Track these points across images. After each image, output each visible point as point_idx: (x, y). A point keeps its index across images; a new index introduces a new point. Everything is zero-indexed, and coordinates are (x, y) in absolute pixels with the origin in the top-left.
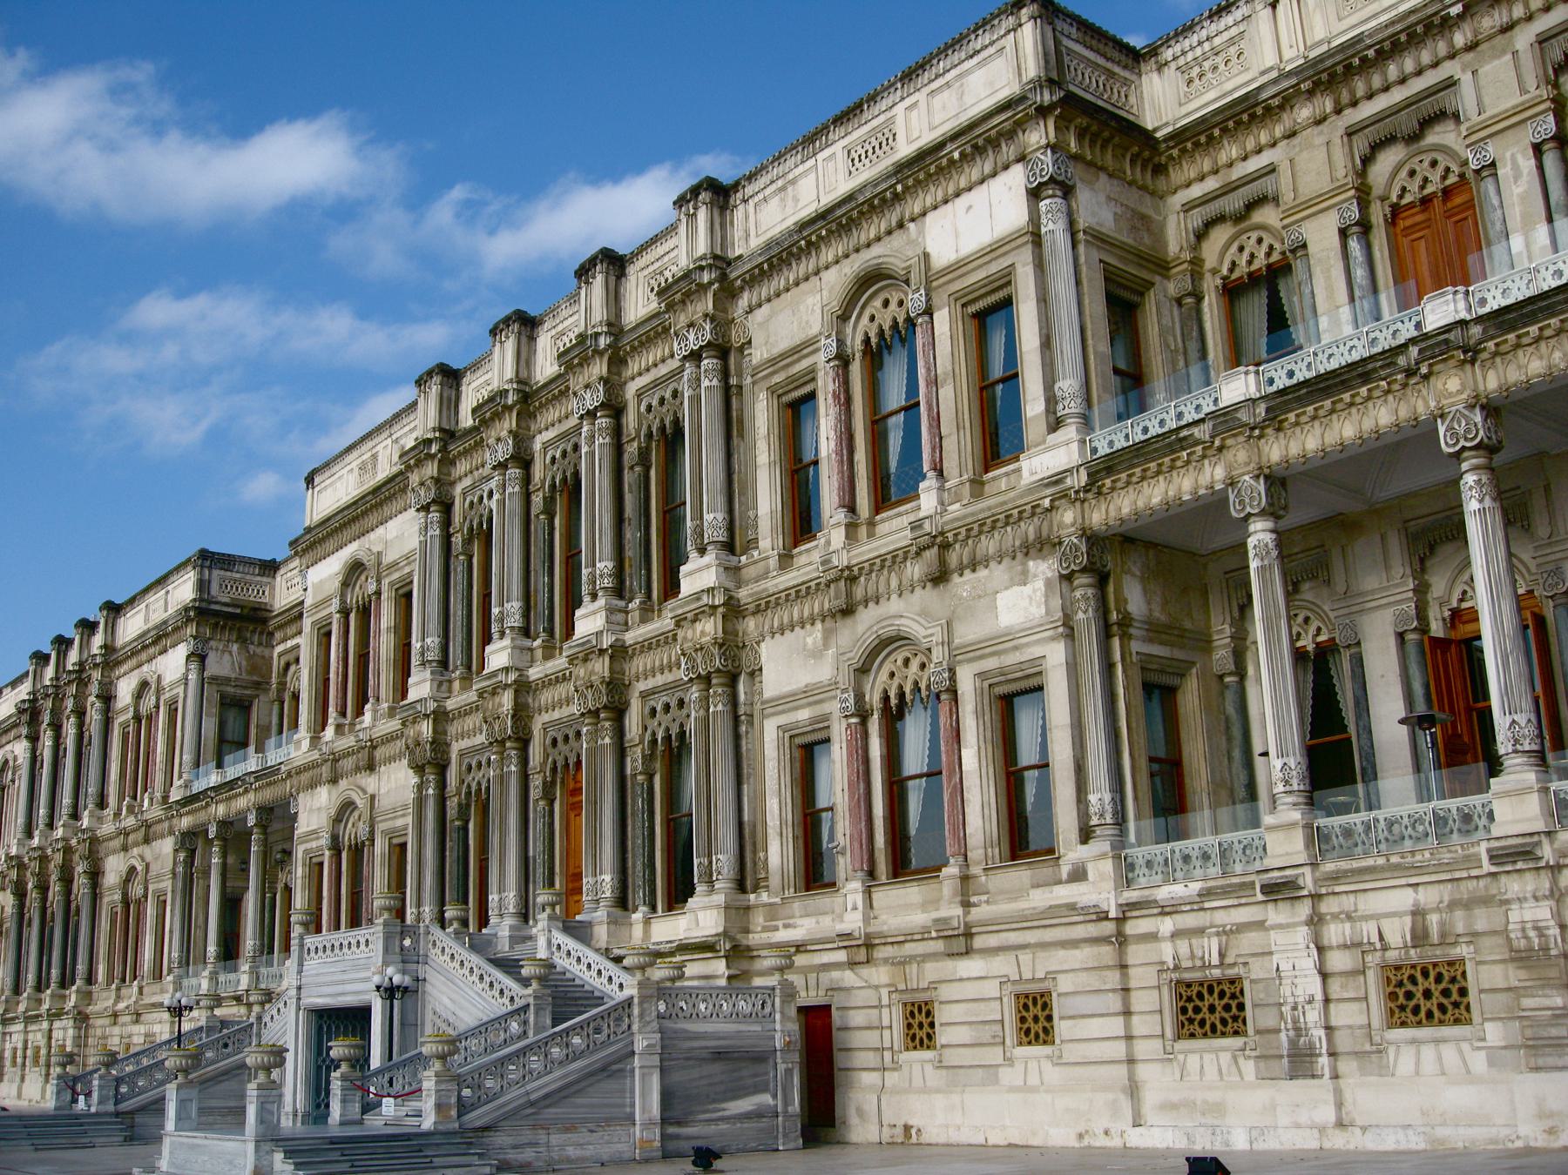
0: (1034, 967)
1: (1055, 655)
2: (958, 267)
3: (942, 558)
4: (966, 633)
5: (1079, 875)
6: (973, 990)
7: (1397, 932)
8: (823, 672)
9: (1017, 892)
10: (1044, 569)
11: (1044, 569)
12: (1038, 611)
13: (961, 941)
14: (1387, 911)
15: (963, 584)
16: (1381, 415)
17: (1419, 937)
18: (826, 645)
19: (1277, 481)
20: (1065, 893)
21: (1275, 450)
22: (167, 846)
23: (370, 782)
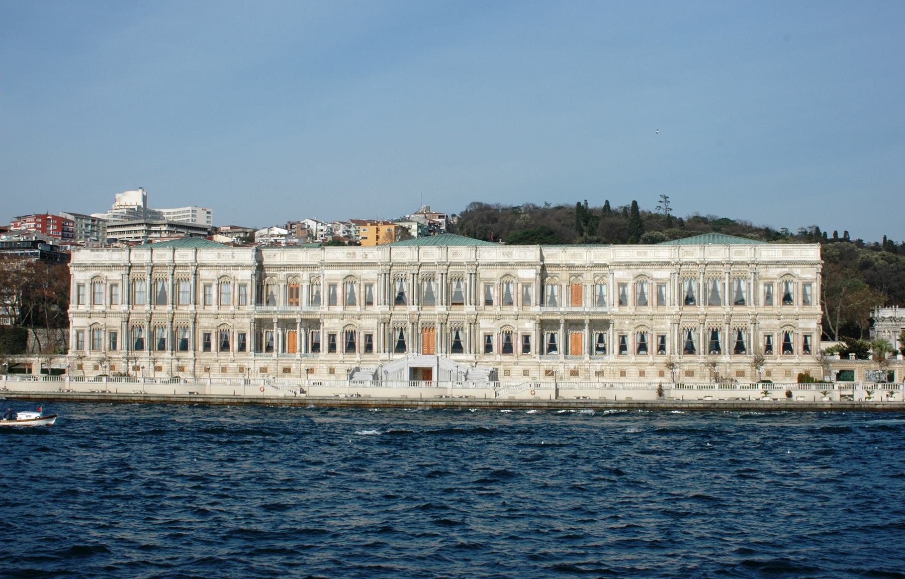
0: (526, 368)
1: (534, 333)
2: (523, 279)
3: (517, 317)
4: (520, 327)
6: (518, 369)
8: (493, 326)
9: (525, 358)
11: (533, 322)
13: (516, 364)
14: (572, 365)
16: (579, 317)
19: (566, 320)
20: (529, 360)
21: (566, 317)
22: (247, 321)
23: (359, 322)
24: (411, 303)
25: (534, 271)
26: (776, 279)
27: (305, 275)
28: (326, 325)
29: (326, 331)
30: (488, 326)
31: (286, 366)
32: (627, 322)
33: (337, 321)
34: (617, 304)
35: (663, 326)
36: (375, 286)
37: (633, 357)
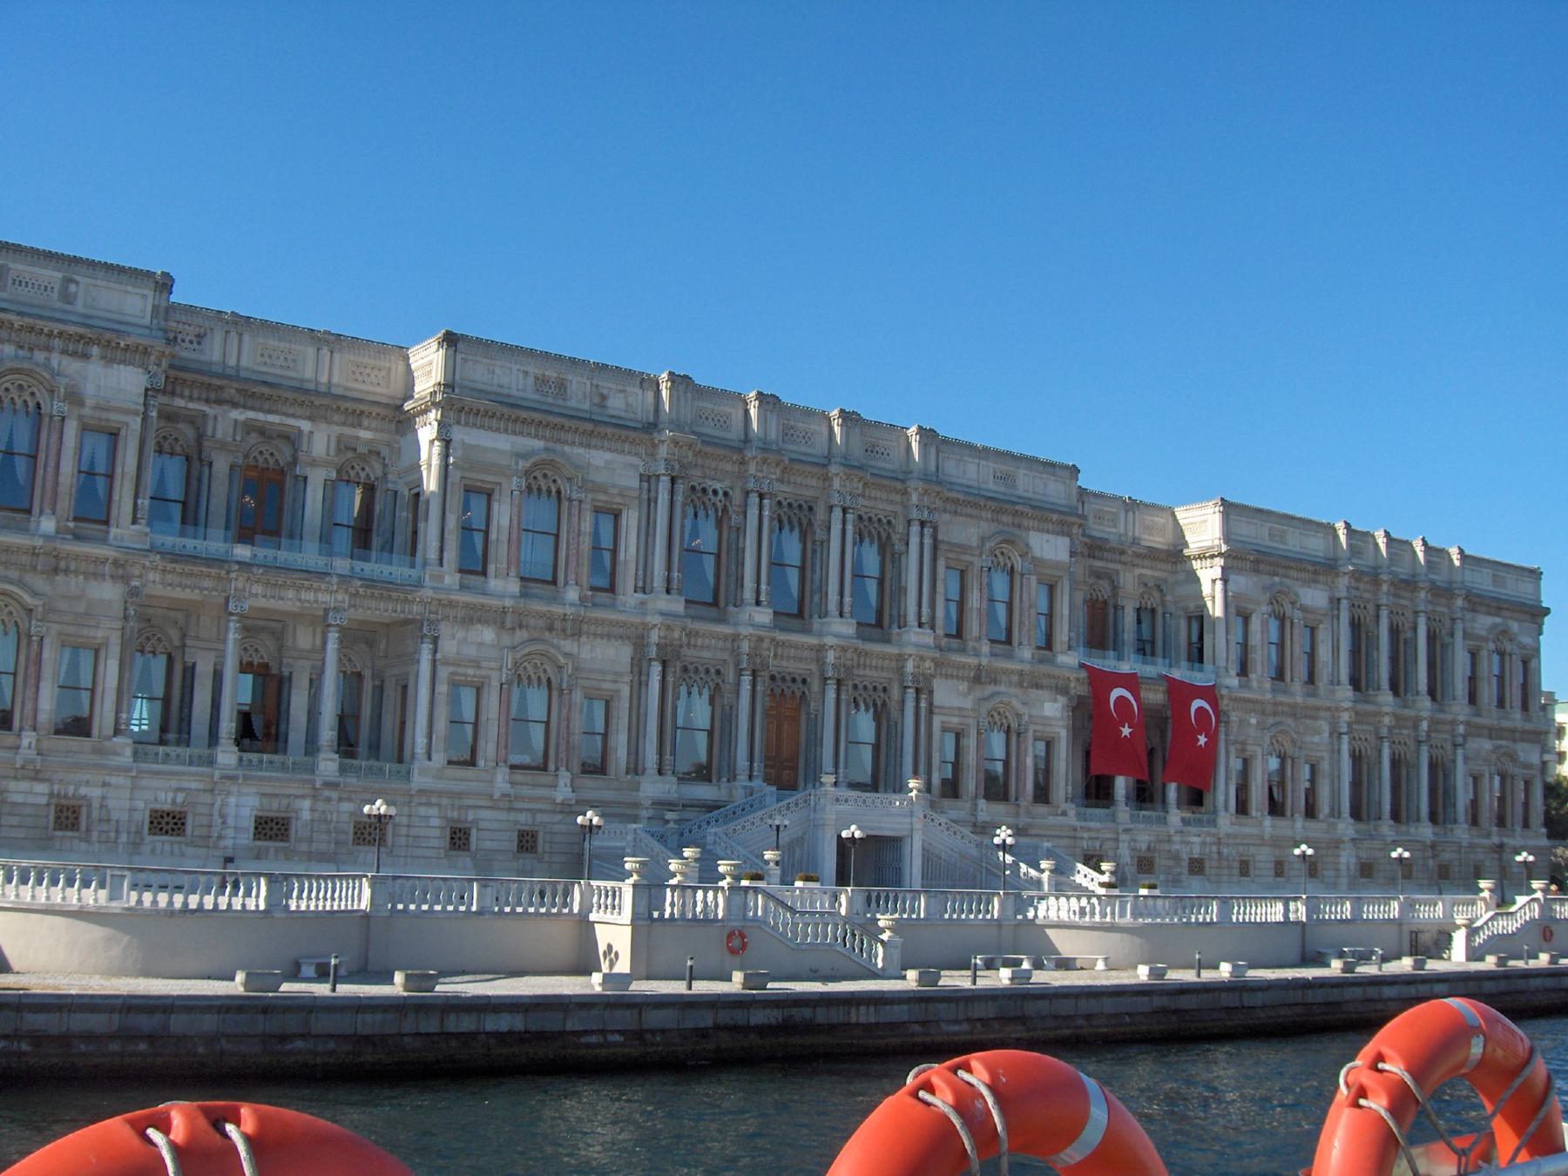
4: (1035, 712)
5: (1064, 814)
7: (1144, 847)
8: (968, 704)
10: (1062, 700)
11: (1062, 700)
12: (1058, 714)
15: (1033, 693)
17: (1149, 849)
18: (969, 693)
24: (748, 594)
25: (1067, 540)
26: (1486, 640)
27: (320, 440)
28: (448, 647)
29: (443, 673)
30: (956, 702)
31: (274, 808)
32: (1253, 721)
33: (488, 634)
34: (1233, 673)
35: (1316, 739)
36: (631, 520)
37: (1268, 821)
